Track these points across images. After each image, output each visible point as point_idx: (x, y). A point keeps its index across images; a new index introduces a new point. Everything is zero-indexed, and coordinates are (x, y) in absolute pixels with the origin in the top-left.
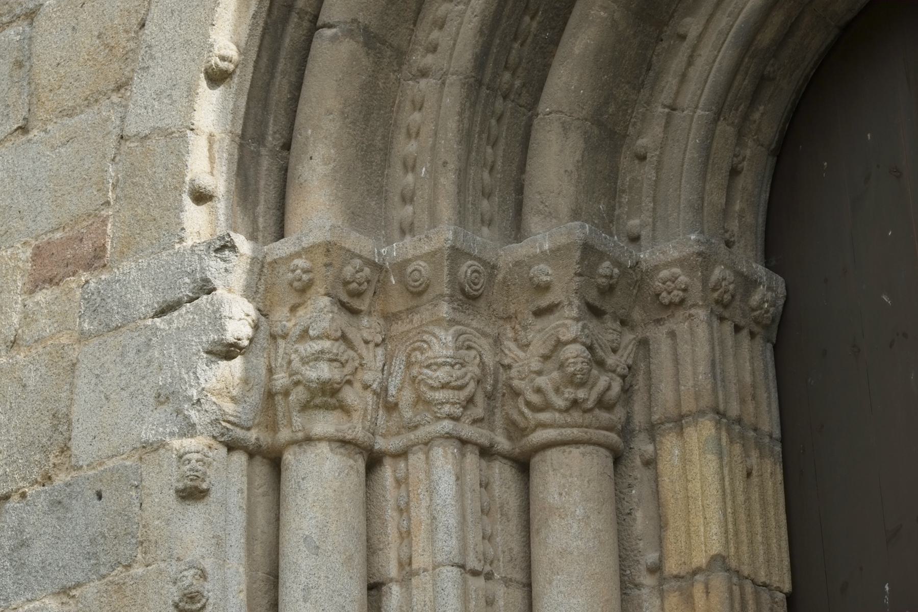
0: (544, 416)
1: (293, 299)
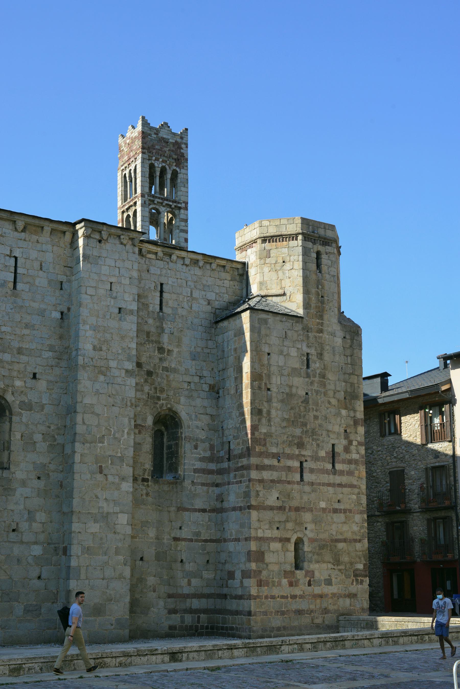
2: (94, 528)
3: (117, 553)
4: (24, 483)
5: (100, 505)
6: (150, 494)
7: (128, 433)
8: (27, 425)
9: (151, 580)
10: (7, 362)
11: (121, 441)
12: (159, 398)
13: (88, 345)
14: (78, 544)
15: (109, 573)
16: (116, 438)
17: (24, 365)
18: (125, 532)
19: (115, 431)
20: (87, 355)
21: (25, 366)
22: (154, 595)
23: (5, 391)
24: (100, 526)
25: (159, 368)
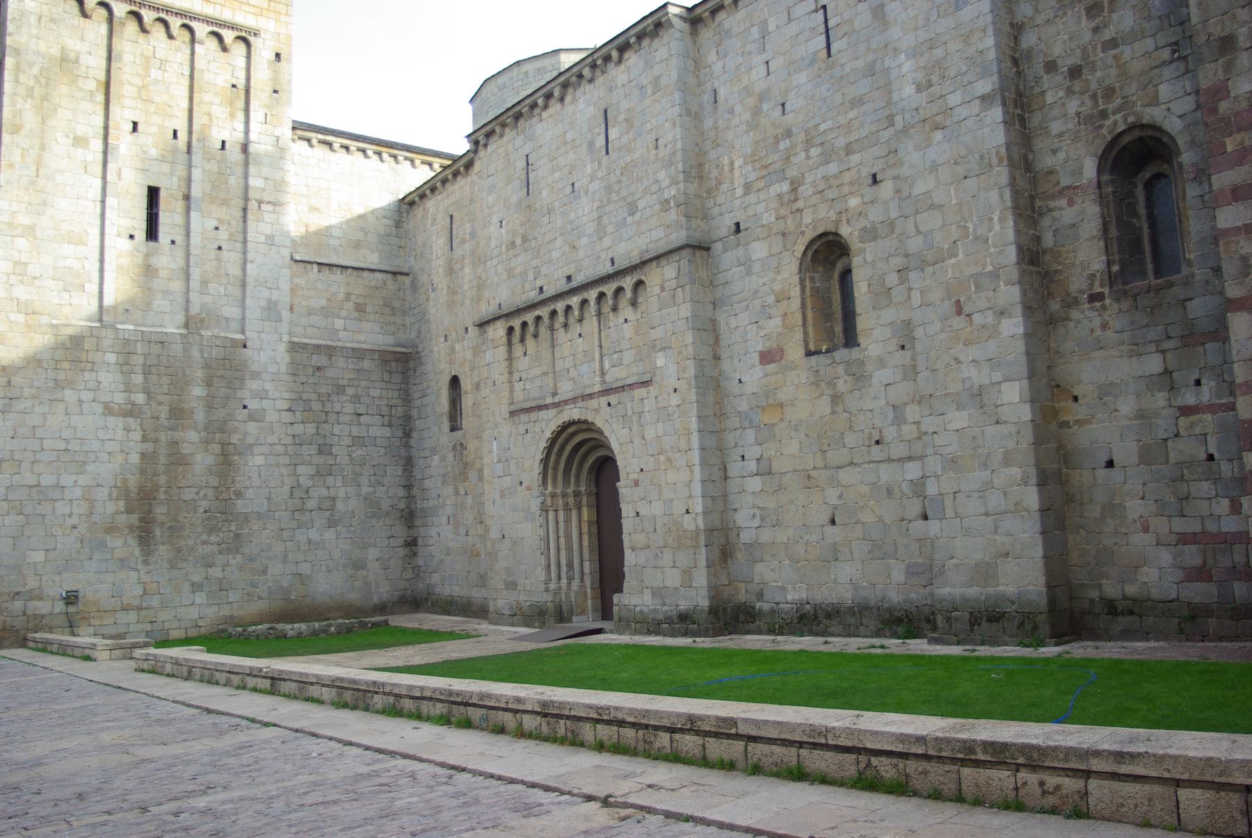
2: (959, 419)
3: (1007, 461)
4: (882, 363)
5: (966, 375)
6: (1111, 324)
7: (1001, 220)
8: (873, 264)
9: (1135, 508)
10: (835, 177)
11: (990, 243)
12: (1104, 114)
13: (907, 89)
14: (936, 454)
15: (995, 501)
16: (977, 238)
17: (856, 169)
18: (1019, 418)
19: (975, 225)
20: (907, 108)
21: (859, 171)
22: (1149, 539)
23: (837, 223)
24: (969, 415)
25: (1095, 48)
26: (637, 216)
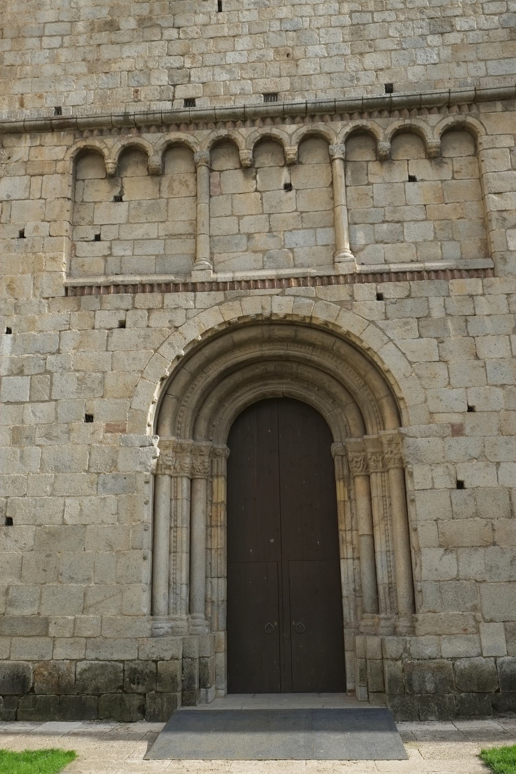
0: (199, 473)
1: (165, 448)
26: (453, 38)
